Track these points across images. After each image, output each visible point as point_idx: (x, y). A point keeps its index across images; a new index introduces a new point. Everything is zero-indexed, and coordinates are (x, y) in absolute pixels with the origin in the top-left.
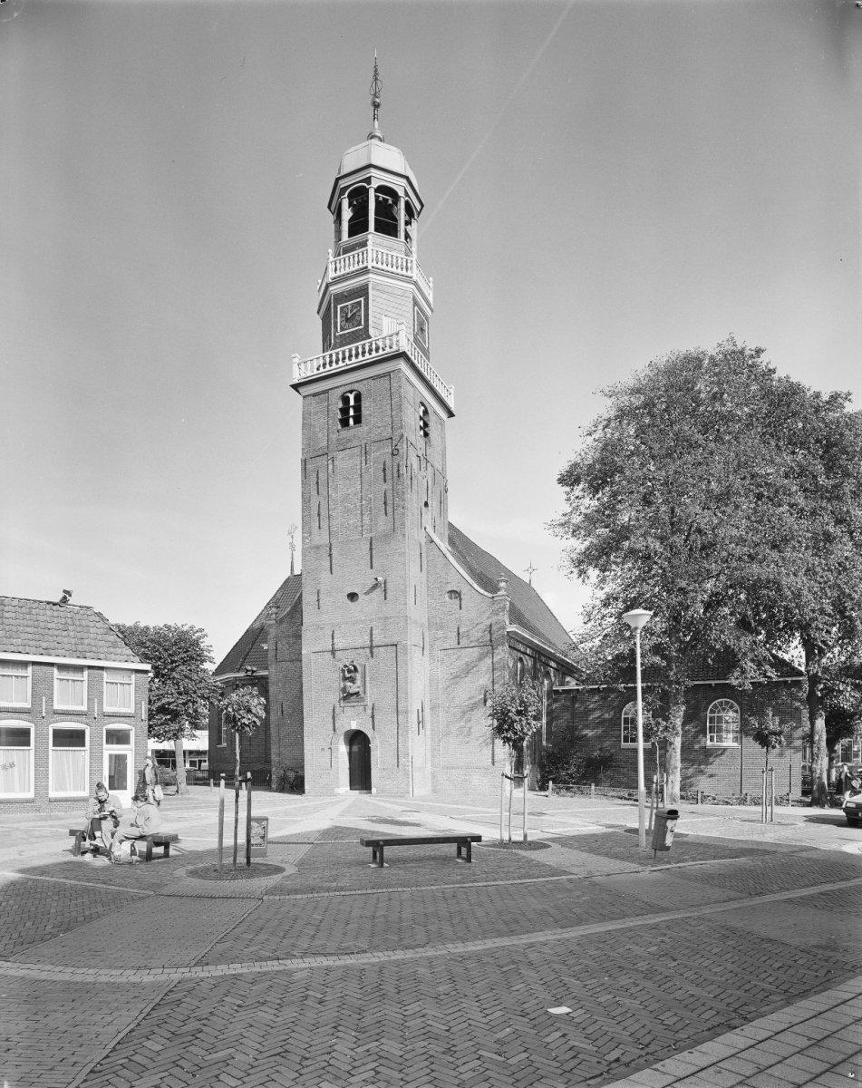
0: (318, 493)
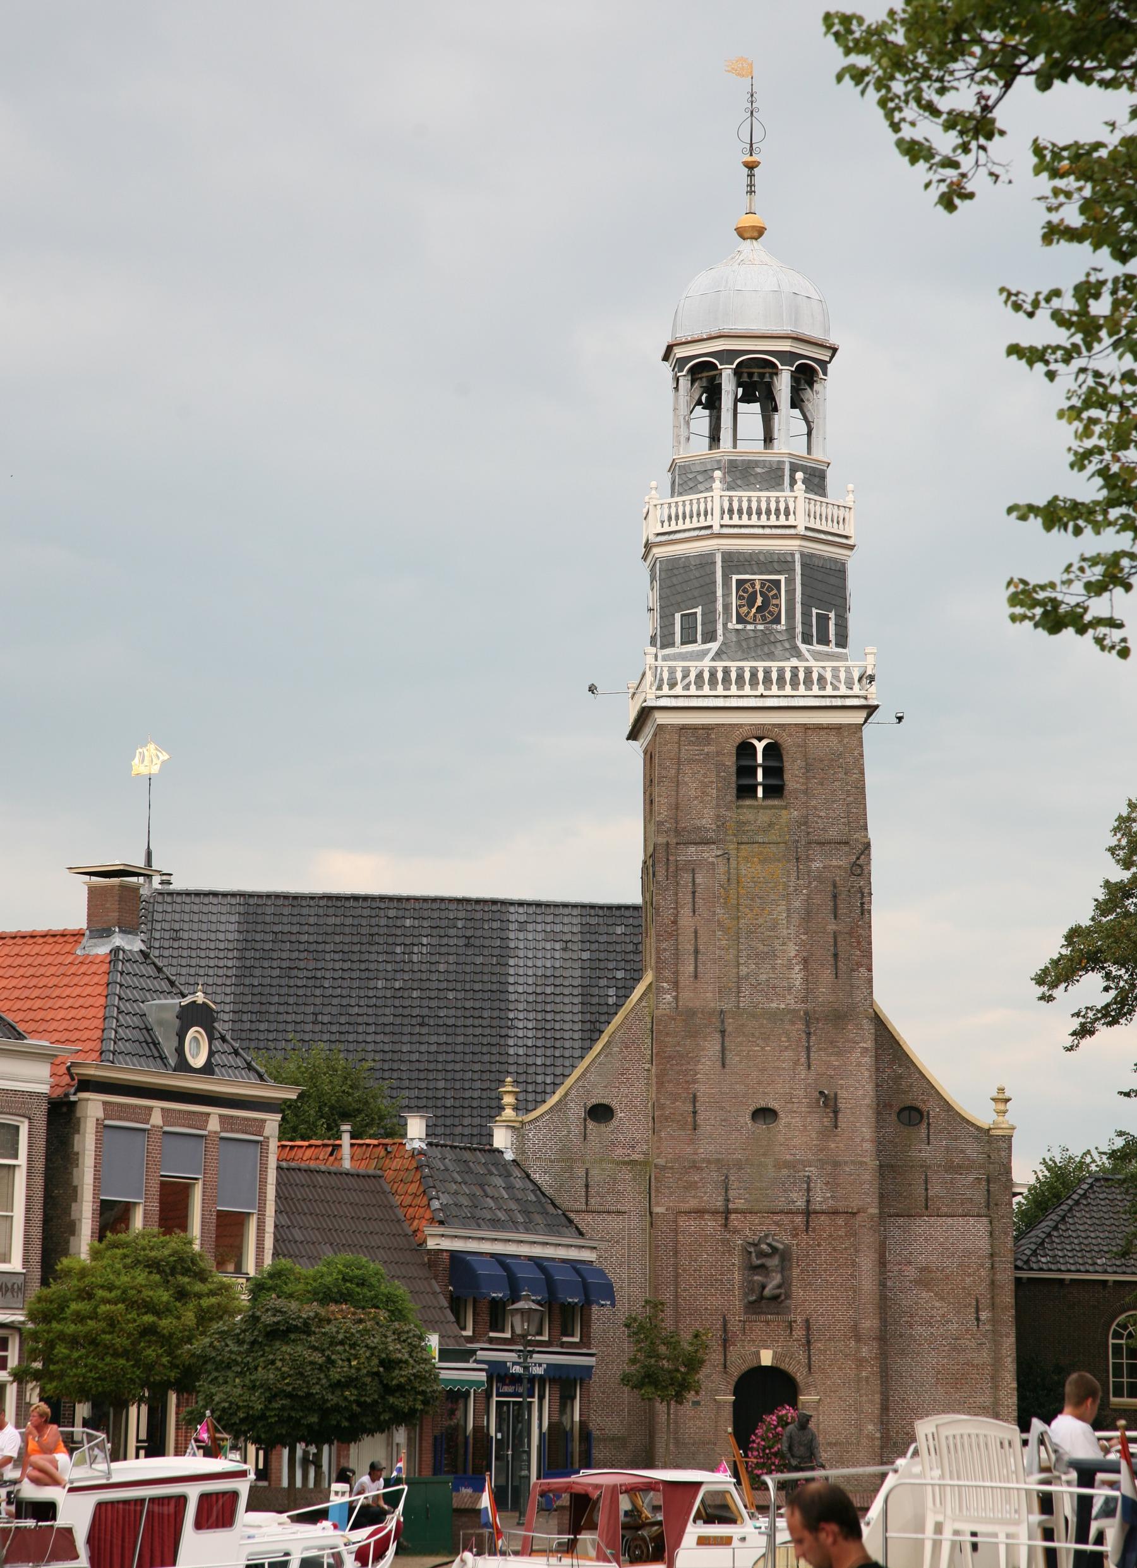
0: (694, 912)
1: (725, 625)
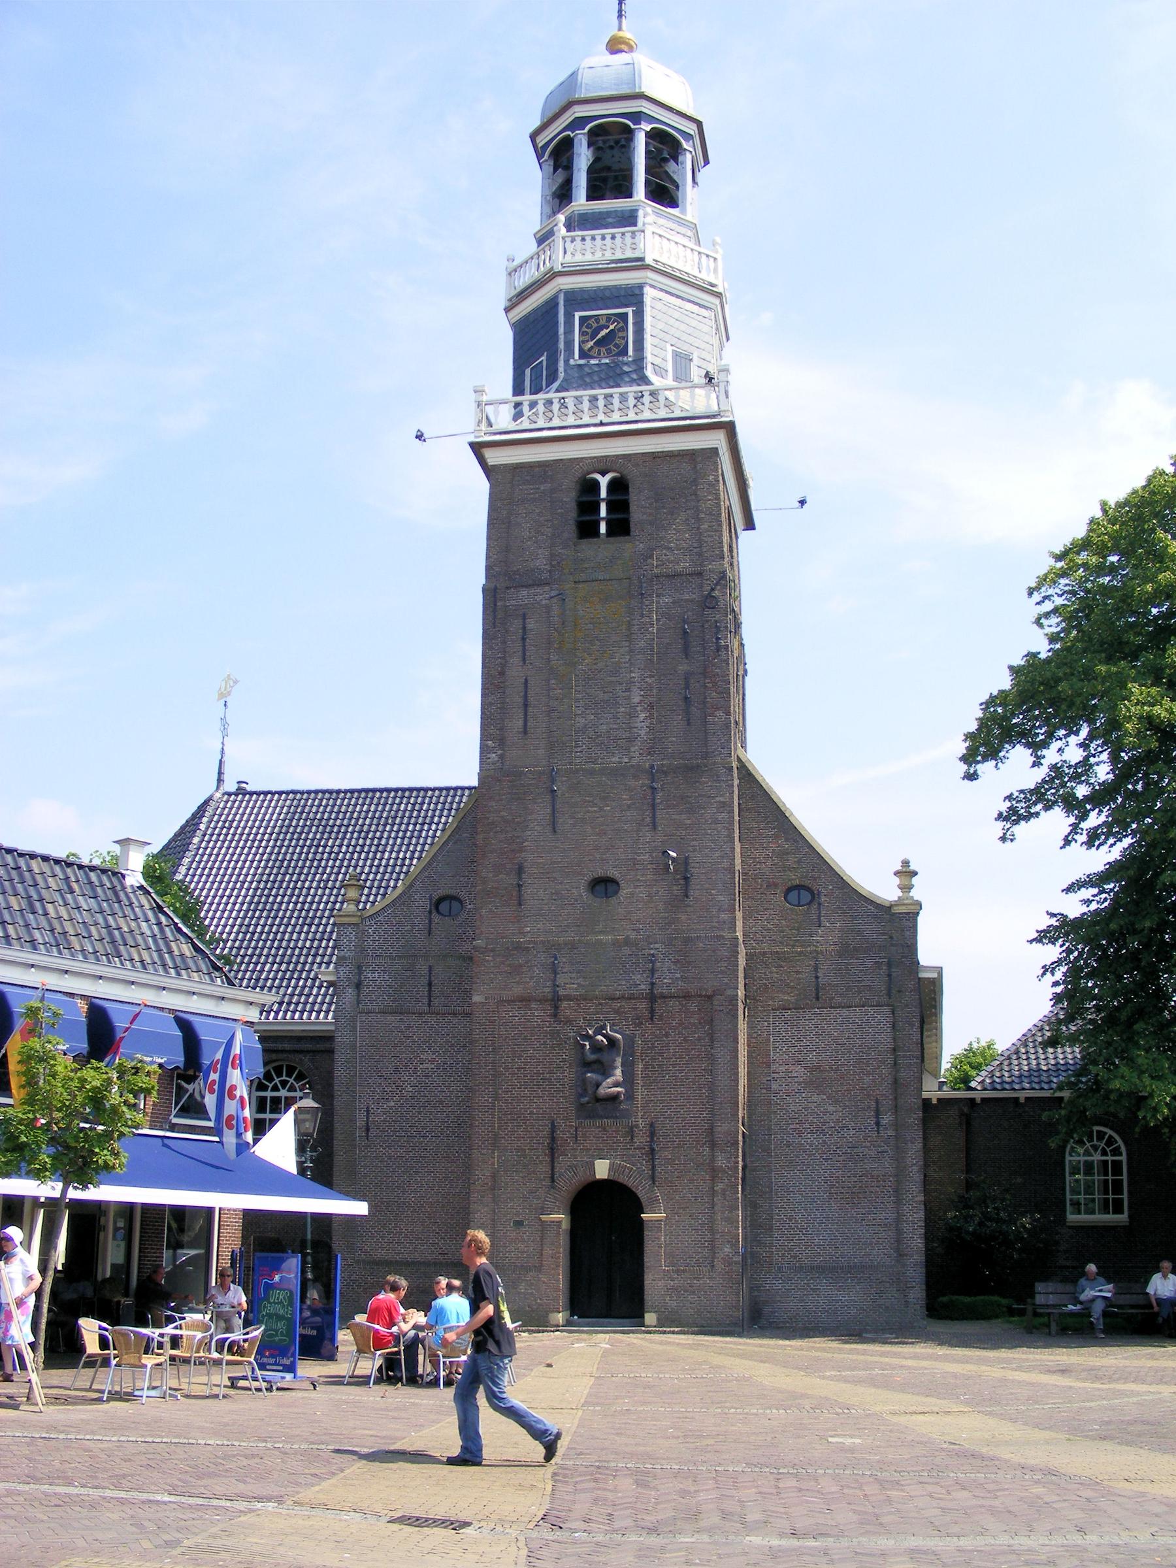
0: (524, 660)
1: (566, 362)
